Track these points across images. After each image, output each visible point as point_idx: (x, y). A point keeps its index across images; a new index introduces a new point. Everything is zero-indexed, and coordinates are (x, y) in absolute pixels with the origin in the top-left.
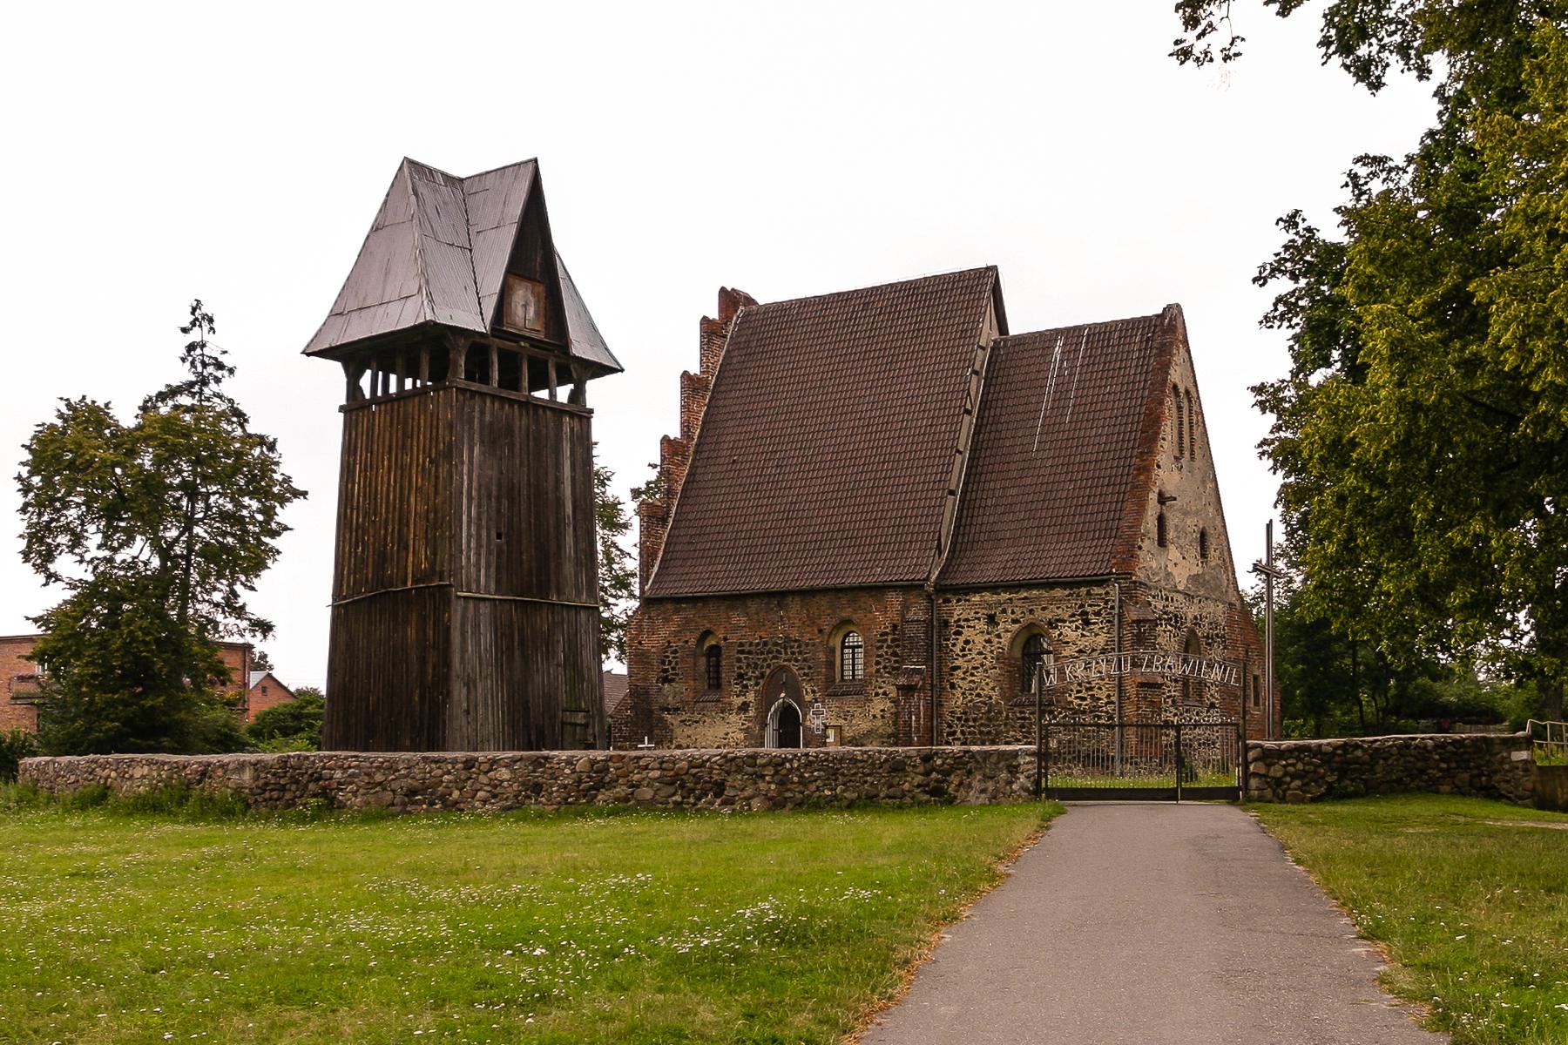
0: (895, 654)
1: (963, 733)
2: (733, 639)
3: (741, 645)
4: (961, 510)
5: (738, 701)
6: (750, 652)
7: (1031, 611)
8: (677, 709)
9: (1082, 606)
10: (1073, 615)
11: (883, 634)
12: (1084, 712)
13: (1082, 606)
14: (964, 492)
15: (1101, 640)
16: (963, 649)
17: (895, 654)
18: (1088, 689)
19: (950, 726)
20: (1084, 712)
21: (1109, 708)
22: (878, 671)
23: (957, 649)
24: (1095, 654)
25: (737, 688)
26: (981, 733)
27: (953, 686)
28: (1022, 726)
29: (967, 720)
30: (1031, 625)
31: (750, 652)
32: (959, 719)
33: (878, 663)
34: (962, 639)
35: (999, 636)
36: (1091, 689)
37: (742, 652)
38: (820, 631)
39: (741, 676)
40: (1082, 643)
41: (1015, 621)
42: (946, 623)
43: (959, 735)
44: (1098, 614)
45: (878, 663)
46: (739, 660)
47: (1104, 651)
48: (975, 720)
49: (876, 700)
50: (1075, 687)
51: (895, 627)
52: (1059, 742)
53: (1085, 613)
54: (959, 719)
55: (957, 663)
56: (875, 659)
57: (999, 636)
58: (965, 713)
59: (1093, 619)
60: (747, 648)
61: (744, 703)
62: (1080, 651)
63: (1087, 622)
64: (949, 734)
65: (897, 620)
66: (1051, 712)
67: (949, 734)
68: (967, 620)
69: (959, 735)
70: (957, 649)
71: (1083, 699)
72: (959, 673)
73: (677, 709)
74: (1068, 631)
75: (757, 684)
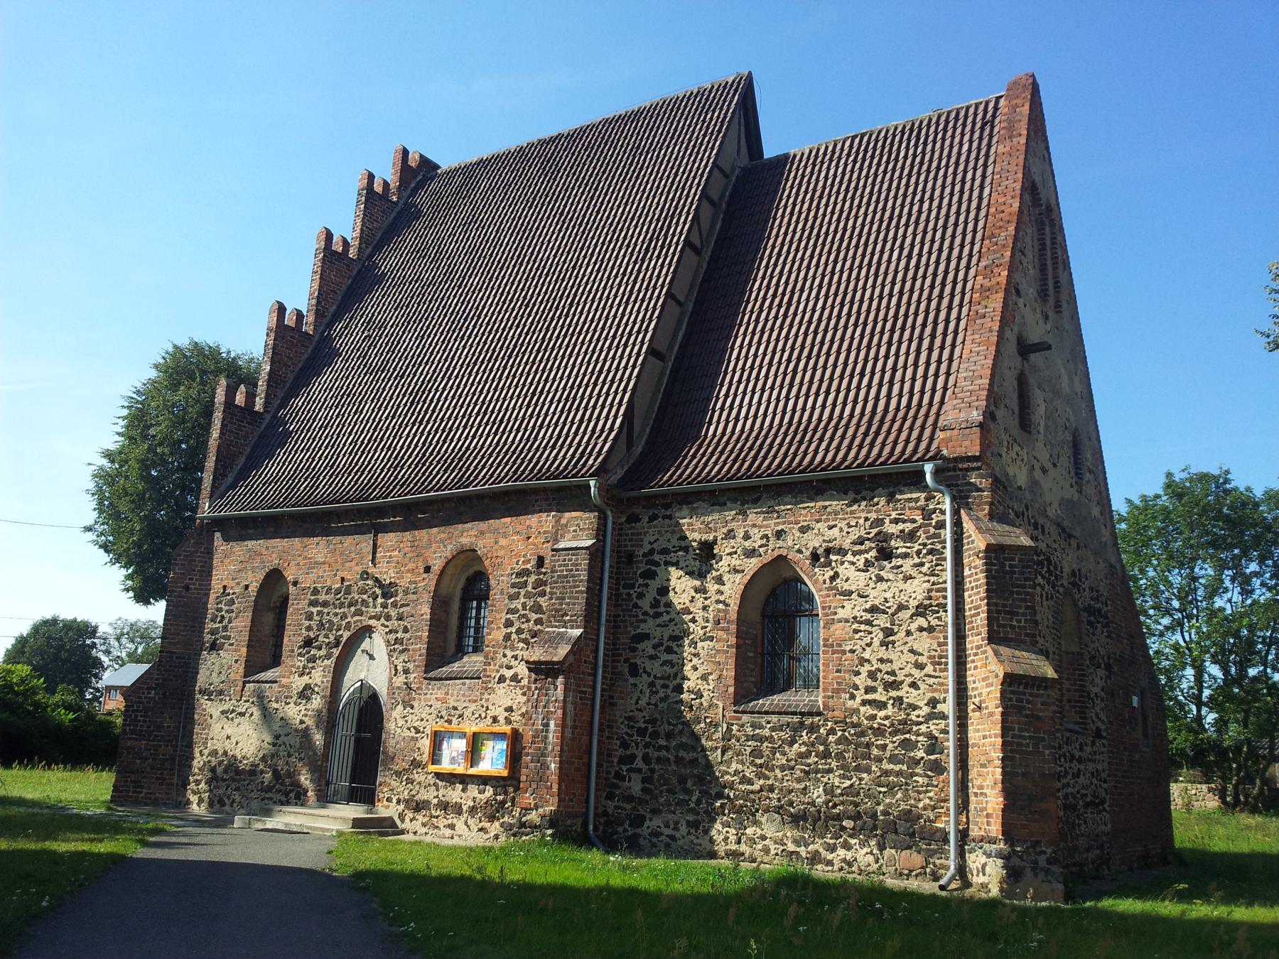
0: (537, 608)
1: (646, 759)
2: (307, 582)
3: (316, 591)
4: (672, 382)
5: (299, 683)
6: (325, 604)
7: (779, 534)
8: (221, 693)
9: (879, 522)
10: (860, 541)
11: (526, 573)
12: (879, 732)
13: (879, 522)
14: (680, 358)
15: (916, 590)
16: (656, 604)
17: (537, 608)
18: (890, 686)
19: (625, 745)
20: (879, 732)
21: (934, 727)
22: (507, 637)
23: (645, 604)
24: (905, 615)
25: (300, 662)
26: (679, 760)
27: (634, 671)
28: (756, 753)
29: (655, 735)
30: (781, 559)
31: (325, 604)
32: (642, 732)
33: (509, 624)
34: (654, 584)
35: (719, 580)
36: (895, 685)
37: (313, 603)
38: (427, 569)
39: (308, 643)
40: (877, 595)
41: (751, 553)
42: (630, 557)
43: (639, 763)
44: (911, 536)
45: (509, 624)
46: (309, 617)
47: (921, 610)
48: (669, 736)
49: (501, 690)
50: (862, 680)
51: (541, 561)
52: (829, 791)
53: (883, 538)
54: (642, 732)
55: (644, 628)
56: (504, 616)
57: (719, 580)
58: (653, 721)
59: (899, 546)
60: (322, 597)
61: (307, 687)
62: (873, 610)
63: (886, 554)
64: (622, 760)
65: (546, 550)
66: (813, 729)
67: (622, 760)
68: (665, 551)
69: (639, 763)
70: (645, 604)
71: (882, 706)
72: (647, 646)
73: (221, 693)
74: (851, 574)
75: (328, 656)
